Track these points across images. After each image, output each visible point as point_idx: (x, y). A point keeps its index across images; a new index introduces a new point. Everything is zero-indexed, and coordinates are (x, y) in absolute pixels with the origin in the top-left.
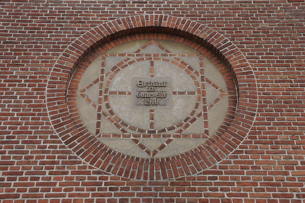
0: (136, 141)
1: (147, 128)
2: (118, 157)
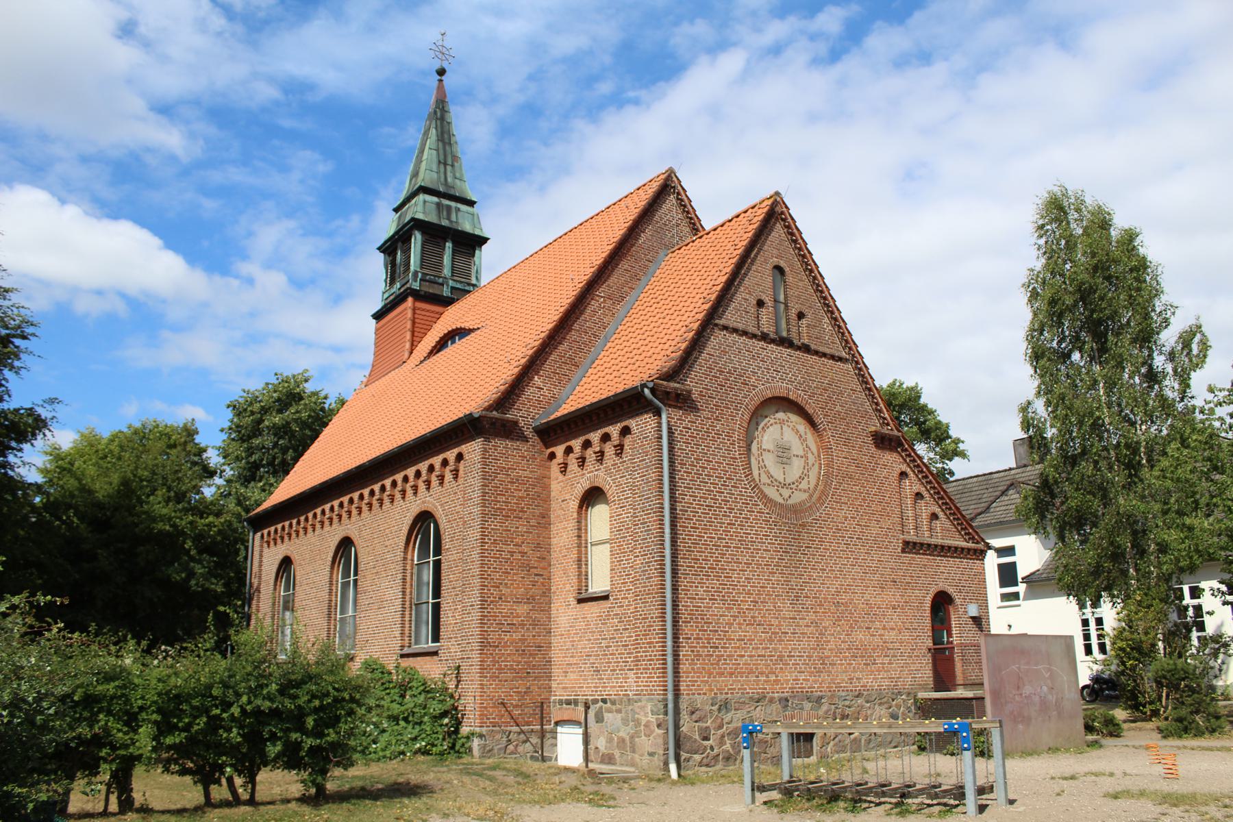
2: (771, 500)
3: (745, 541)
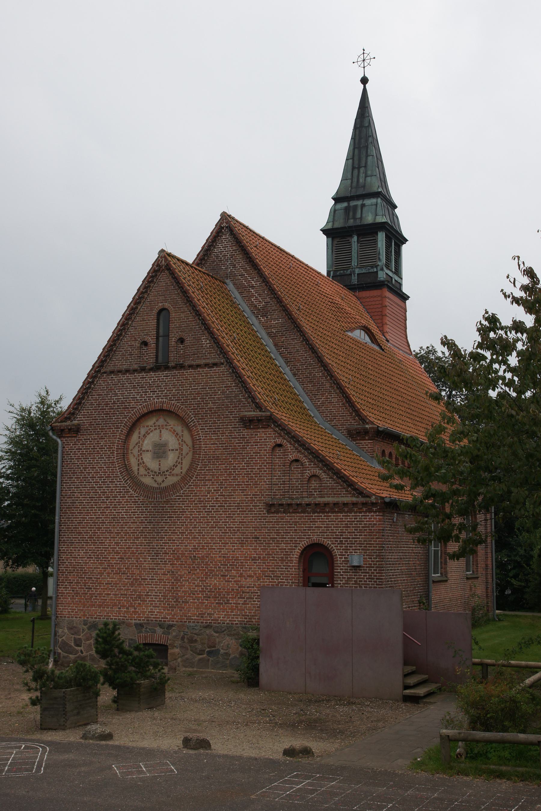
0: (153, 478)
1: (158, 471)
2: (147, 486)
3: (117, 518)
